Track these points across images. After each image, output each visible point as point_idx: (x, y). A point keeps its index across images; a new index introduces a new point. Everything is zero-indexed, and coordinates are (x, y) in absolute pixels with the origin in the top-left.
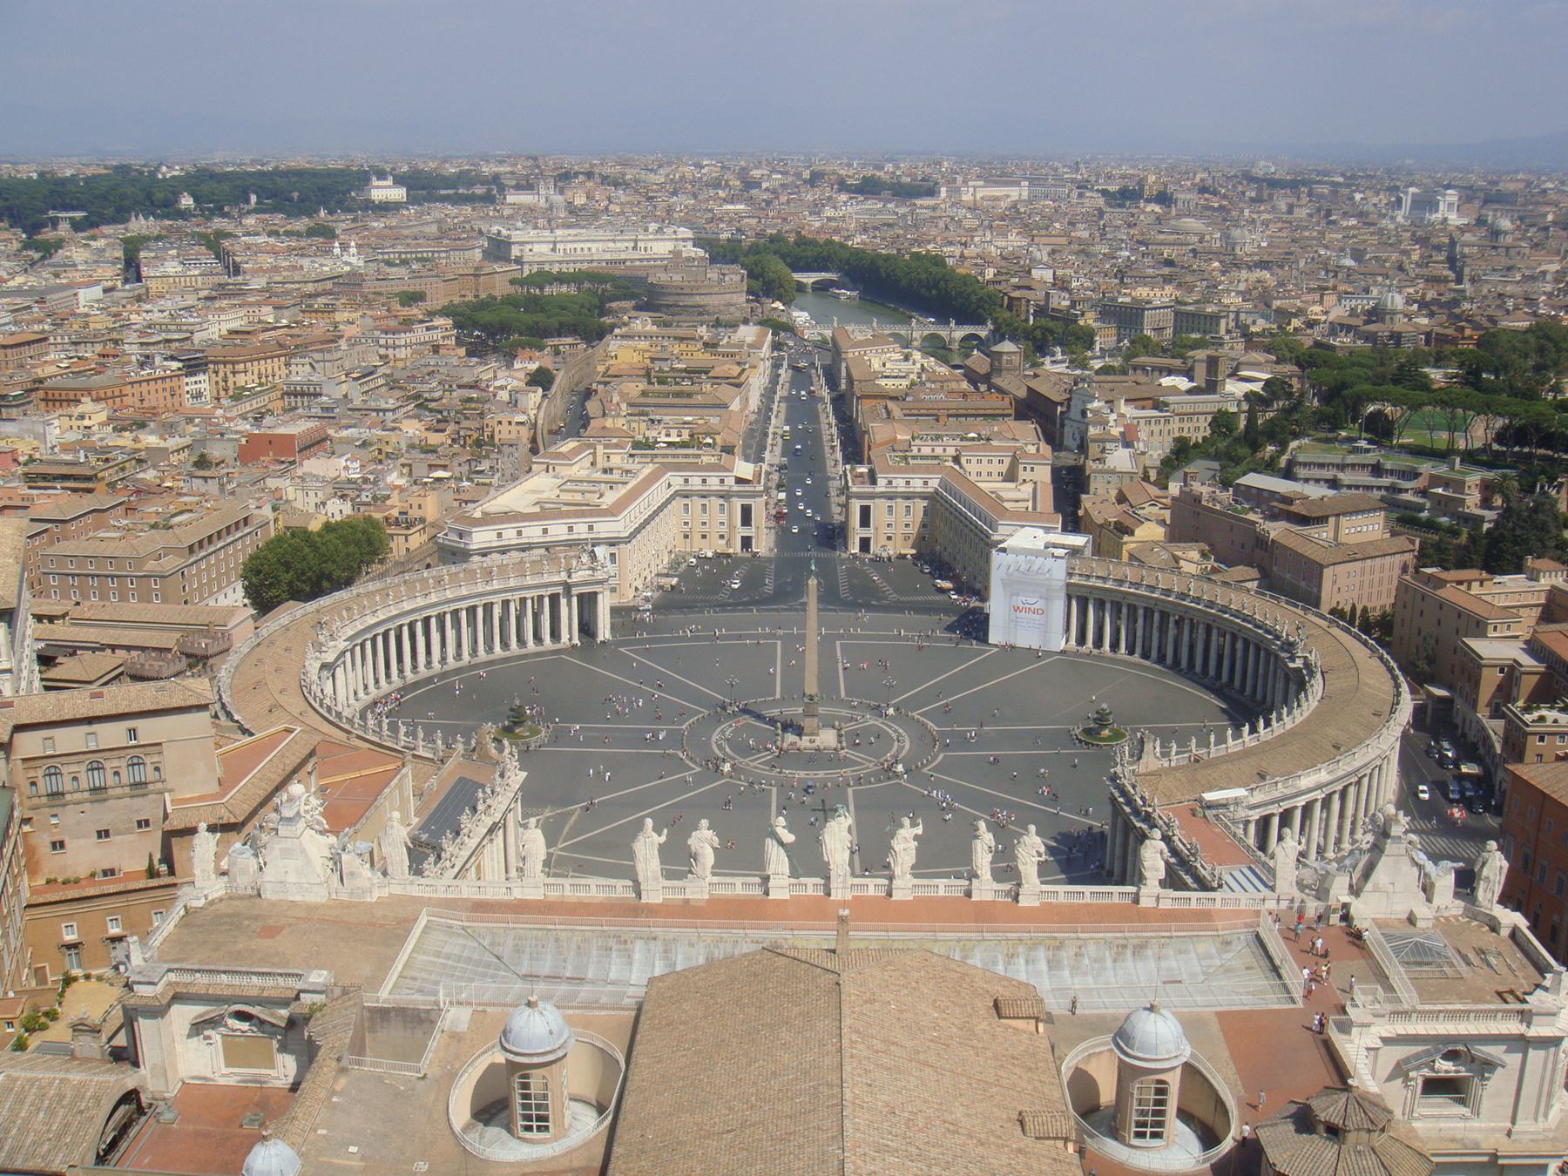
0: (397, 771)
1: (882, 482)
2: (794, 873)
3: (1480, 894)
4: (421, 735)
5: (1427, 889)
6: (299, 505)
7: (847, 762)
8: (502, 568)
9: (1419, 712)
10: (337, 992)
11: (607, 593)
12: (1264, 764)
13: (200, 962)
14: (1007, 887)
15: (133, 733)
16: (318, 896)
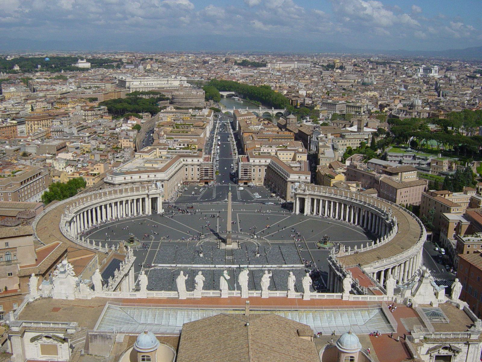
0: (93, 257)
1: (251, 160)
2: (229, 289)
3: (453, 296)
4: (100, 244)
5: (436, 294)
6: (57, 168)
8: (126, 190)
9: (429, 237)
10: (80, 329)
11: (161, 197)
12: (379, 254)
13: (33, 319)
14: (299, 294)
15: (7, 244)
16: (72, 298)
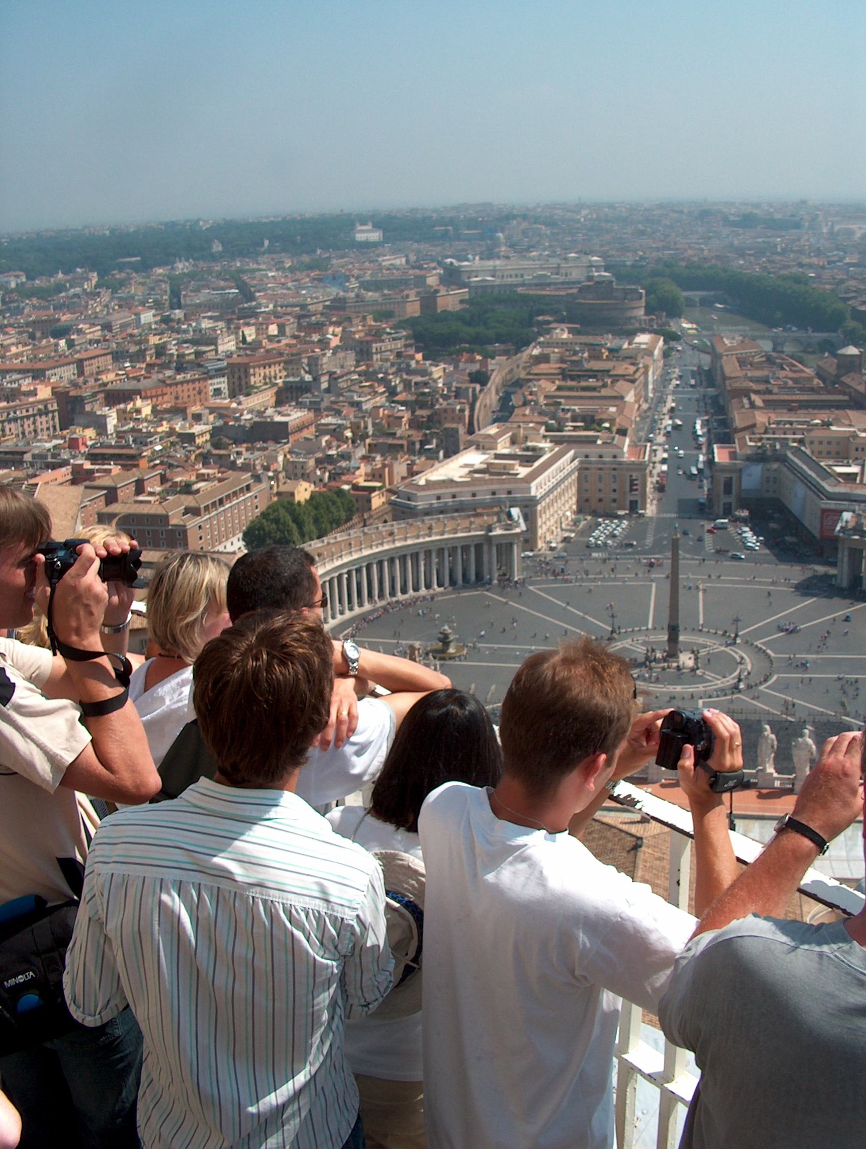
7: (702, 679)
